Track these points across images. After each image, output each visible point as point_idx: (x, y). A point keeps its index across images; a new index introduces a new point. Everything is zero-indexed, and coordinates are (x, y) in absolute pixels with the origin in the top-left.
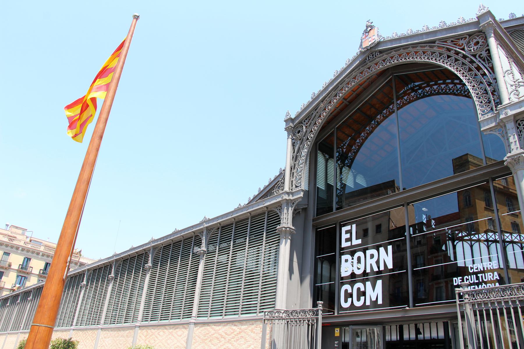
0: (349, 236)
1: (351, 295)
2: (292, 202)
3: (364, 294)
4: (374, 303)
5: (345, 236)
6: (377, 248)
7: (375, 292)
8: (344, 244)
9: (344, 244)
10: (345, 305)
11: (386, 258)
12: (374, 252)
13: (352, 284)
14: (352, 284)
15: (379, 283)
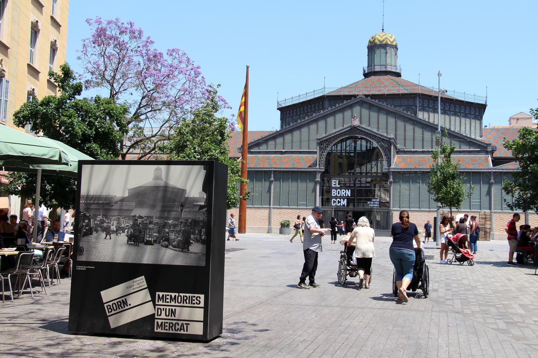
0: (335, 183)
1: (336, 202)
2: (320, 171)
3: (340, 202)
4: (344, 205)
5: (333, 183)
6: (346, 189)
7: (344, 202)
8: (333, 186)
9: (333, 186)
10: (333, 205)
11: (349, 193)
12: (344, 190)
13: (336, 199)
14: (336, 199)
15: (346, 200)
